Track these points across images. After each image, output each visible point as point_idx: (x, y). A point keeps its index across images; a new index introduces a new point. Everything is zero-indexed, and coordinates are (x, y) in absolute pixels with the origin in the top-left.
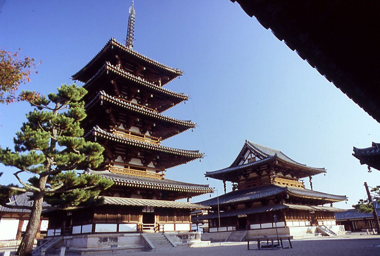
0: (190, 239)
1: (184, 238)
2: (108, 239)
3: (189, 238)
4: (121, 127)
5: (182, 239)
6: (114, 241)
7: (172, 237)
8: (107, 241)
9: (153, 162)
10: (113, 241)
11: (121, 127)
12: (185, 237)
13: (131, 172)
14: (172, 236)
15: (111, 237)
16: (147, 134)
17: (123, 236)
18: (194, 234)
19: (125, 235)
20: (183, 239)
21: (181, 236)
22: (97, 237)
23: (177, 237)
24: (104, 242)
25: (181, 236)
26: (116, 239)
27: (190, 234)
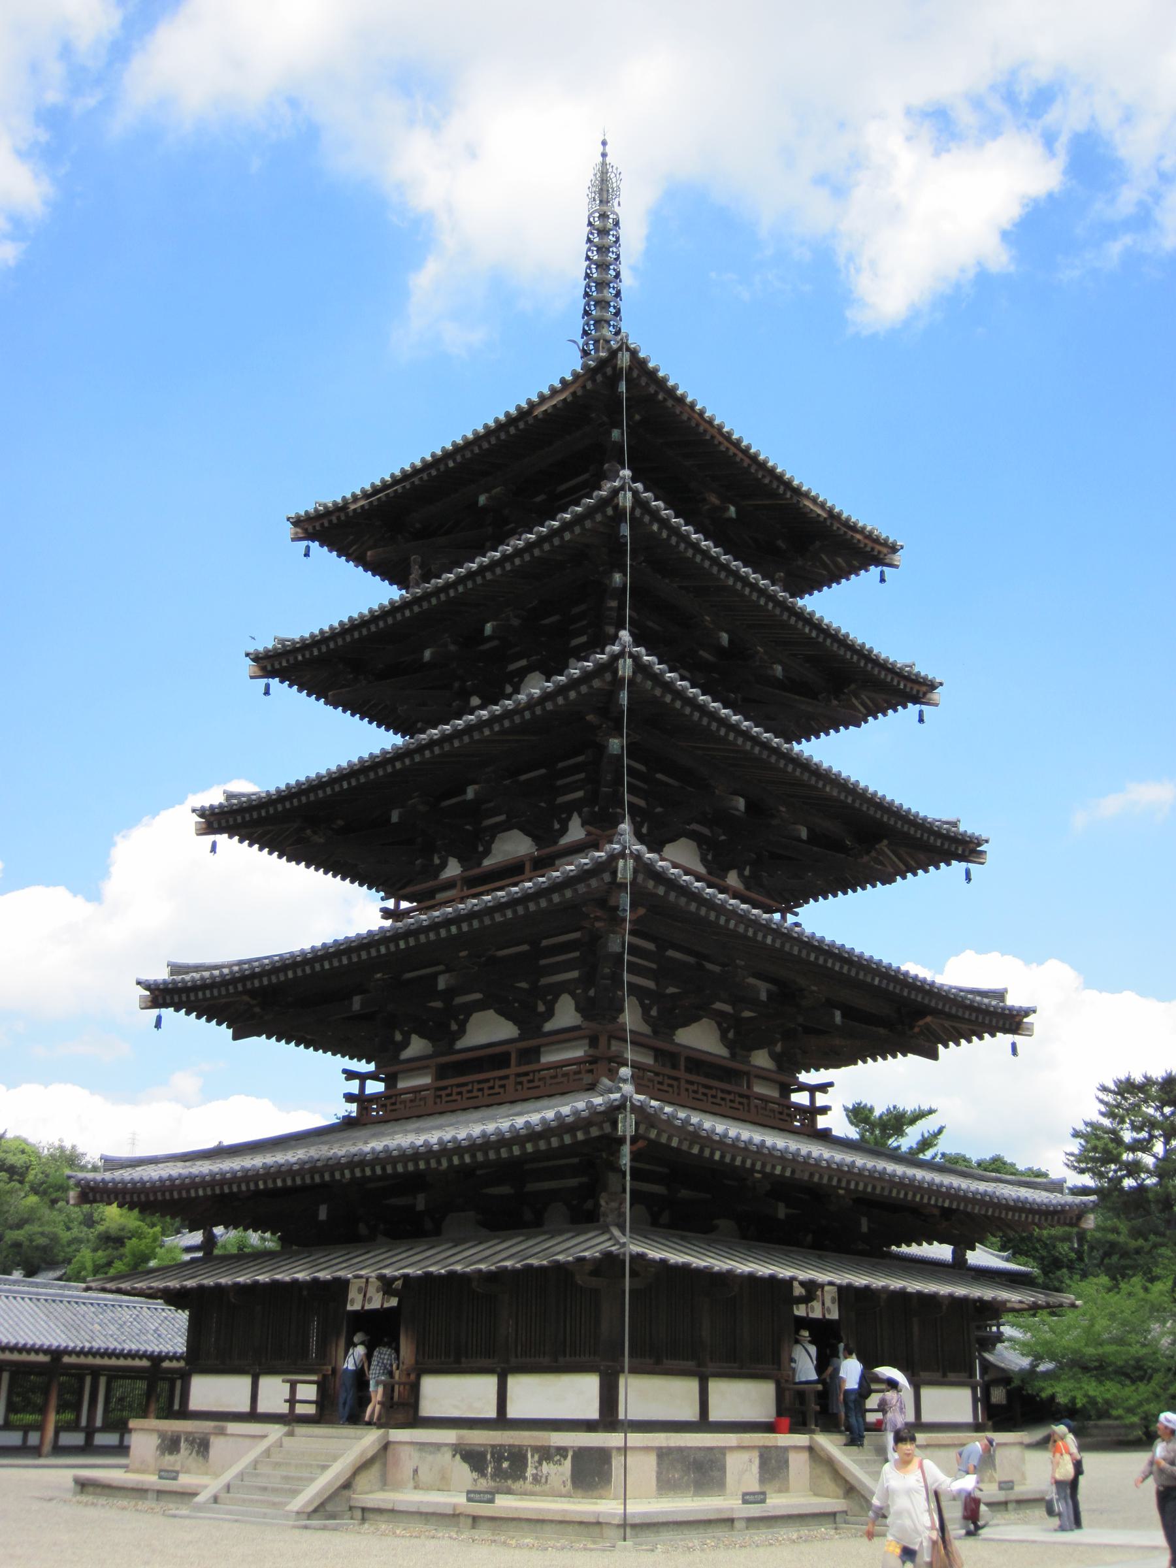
0: (536, 1479)
1: (499, 1474)
2: (183, 1445)
3: (530, 1471)
4: (453, 869)
5: (483, 1474)
6: (198, 1453)
7: (430, 1458)
8: (178, 1451)
9: (573, 995)
10: (194, 1453)
11: (453, 869)
12: (505, 1465)
13: (443, 1093)
14: (431, 1453)
15: (191, 1433)
16: (576, 832)
17: (222, 1432)
18: (562, 1451)
19: (229, 1431)
20: (494, 1476)
21: (482, 1455)
22: (153, 1430)
23: (458, 1457)
24: (171, 1453)
25: (482, 1455)
26: (202, 1446)
27: (536, 1449)
